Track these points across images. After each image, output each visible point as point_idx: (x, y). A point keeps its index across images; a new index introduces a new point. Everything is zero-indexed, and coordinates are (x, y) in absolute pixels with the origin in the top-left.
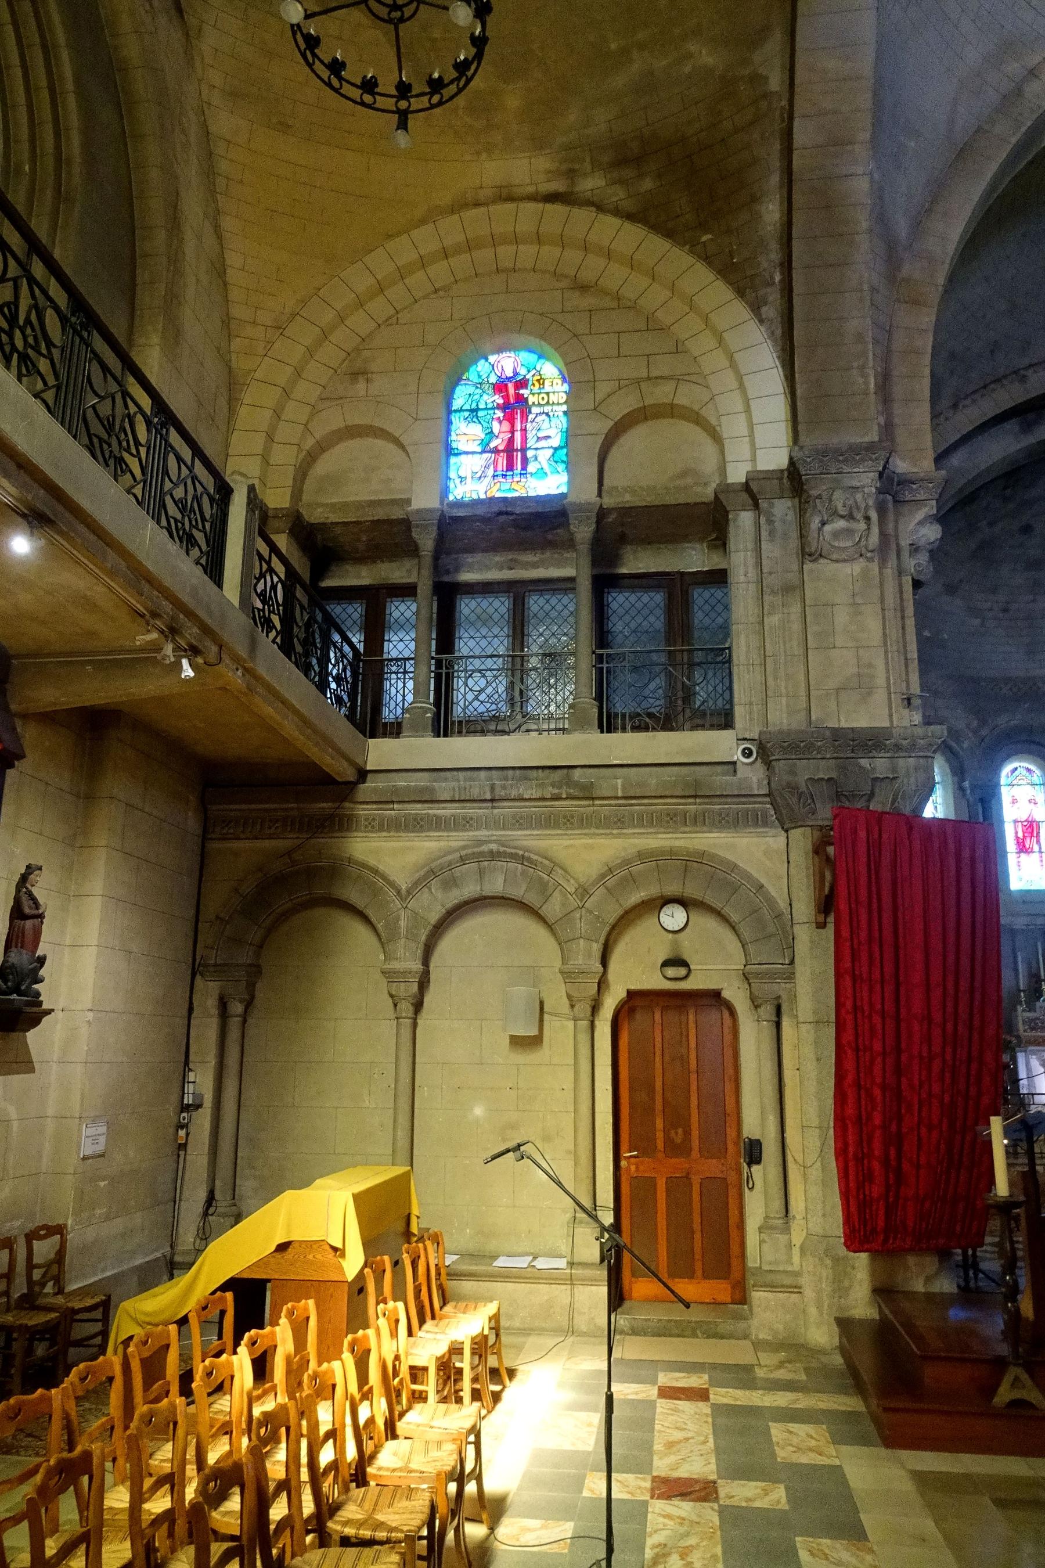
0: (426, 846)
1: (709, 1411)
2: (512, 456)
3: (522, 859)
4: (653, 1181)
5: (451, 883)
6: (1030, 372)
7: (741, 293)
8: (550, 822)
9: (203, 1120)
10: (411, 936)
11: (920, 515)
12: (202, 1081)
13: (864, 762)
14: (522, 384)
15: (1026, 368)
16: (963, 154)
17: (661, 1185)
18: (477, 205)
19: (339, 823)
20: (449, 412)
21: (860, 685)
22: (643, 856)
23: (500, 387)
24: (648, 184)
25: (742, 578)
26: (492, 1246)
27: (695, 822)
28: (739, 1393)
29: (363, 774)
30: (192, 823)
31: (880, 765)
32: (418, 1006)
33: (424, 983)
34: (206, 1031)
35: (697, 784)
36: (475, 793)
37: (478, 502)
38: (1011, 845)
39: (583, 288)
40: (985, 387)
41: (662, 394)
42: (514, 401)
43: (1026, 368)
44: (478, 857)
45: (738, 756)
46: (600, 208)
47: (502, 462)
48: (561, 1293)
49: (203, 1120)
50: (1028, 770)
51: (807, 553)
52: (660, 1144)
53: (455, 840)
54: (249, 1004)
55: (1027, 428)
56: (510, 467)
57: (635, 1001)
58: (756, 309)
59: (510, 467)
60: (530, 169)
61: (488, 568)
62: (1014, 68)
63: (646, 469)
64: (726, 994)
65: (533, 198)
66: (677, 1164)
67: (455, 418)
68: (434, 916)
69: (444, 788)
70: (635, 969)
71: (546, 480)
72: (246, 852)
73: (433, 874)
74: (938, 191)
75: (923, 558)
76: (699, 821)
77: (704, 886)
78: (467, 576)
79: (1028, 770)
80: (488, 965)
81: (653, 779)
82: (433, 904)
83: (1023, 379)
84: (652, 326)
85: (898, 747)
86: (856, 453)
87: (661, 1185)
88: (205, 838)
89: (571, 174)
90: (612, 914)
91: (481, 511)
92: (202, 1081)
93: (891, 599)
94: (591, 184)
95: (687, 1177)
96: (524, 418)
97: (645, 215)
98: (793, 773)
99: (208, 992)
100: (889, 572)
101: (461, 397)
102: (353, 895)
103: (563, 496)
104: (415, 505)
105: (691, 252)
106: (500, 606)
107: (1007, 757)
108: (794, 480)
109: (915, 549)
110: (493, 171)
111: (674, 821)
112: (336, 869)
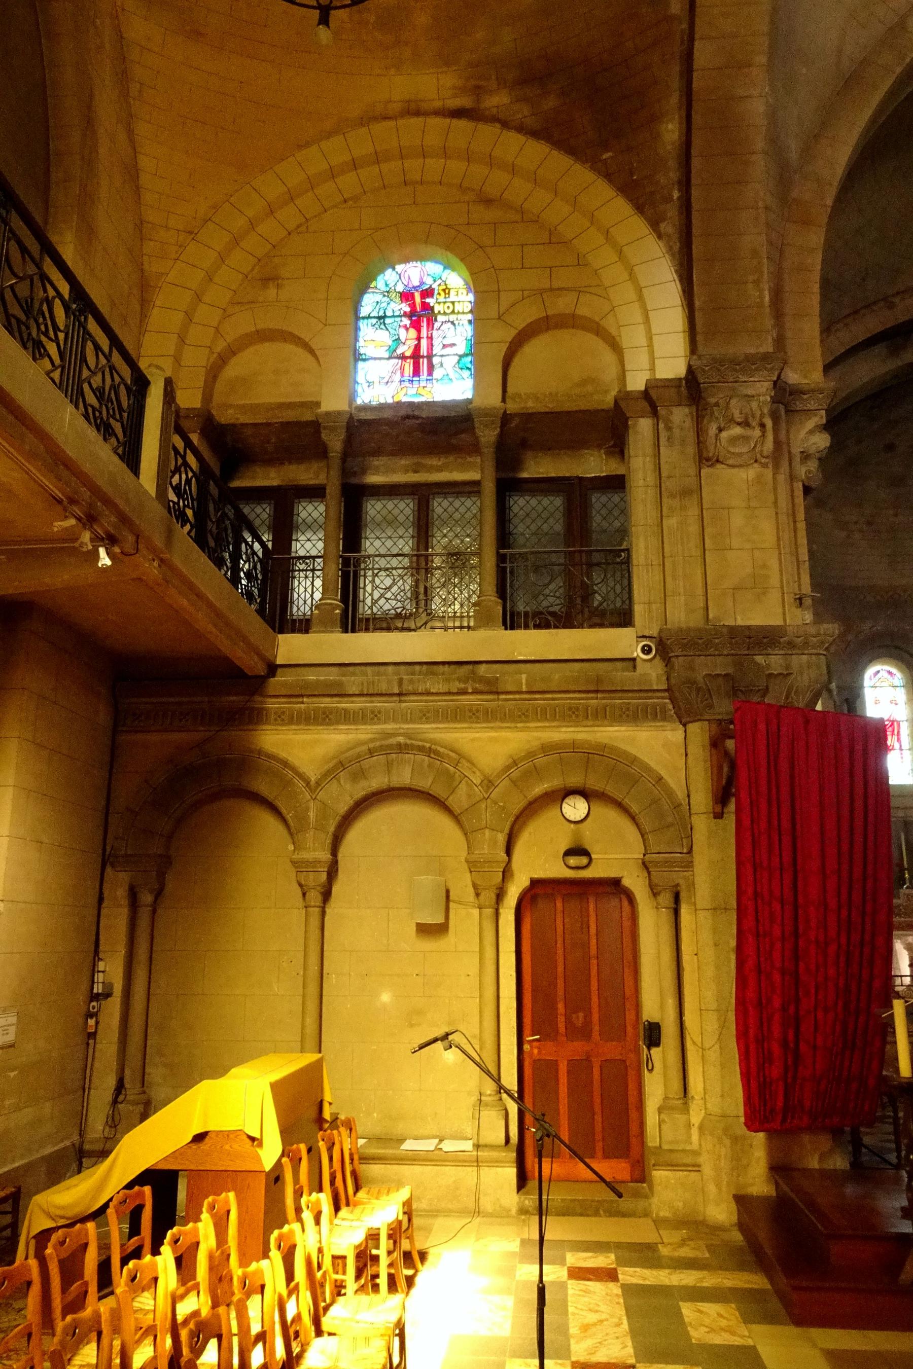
0: (334, 739)
1: (619, 1291)
2: (419, 361)
3: (429, 752)
4: (553, 1066)
5: (359, 775)
6: (897, 300)
7: (640, 209)
8: (457, 716)
9: (112, 1009)
10: (320, 828)
11: (811, 424)
12: (112, 970)
13: (759, 659)
14: (428, 293)
15: (893, 296)
16: (851, 82)
17: (563, 1067)
18: (386, 118)
19: (252, 717)
20: (357, 318)
21: (755, 585)
22: (547, 749)
23: (406, 296)
24: (551, 103)
25: (641, 483)
26: (400, 1128)
27: (596, 716)
28: (647, 1272)
29: (273, 669)
30: (103, 717)
31: (774, 661)
32: (327, 895)
33: (333, 871)
34: (116, 921)
35: (599, 680)
36: (384, 688)
37: (382, 407)
39: (488, 202)
40: (856, 312)
41: (563, 305)
42: (420, 310)
43: (893, 296)
44: (386, 750)
45: (638, 653)
46: (505, 125)
47: (409, 367)
48: (468, 1174)
49: (112, 1009)
50: (890, 673)
51: (705, 458)
52: (562, 1029)
53: (363, 733)
54: (159, 894)
55: (894, 352)
56: (416, 372)
57: (538, 889)
58: (654, 225)
59: (416, 372)
60: (437, 85)
61: (394, 471)
63: (551, 375)
64: (626, 882)
65: (438, 113)
66: (577, 1048)
67: (362, 324)
68: (343, 808)
69: (353, 682)
70: (539, 857)
71: (452, 384)
72: (156, 745)
73: (342, 766)
75: (813, 465)
76: (601, 716)
78: (374, 479)
79: (890, 673)
80: (395, 854)
81: (557, 674)
83: (891, 306)
84: (554, 239)
85: (791, 645)
87: (563, 1067)
88: (115, 731)
89: (478, 91)
90: (517, 804)
91: (387, 414)
92: (112, 970)
93: (783, 503)
95: (588, 1060)
96: (430, 324)
97: (545, 132)
98: (691, 668)
99: (118, 885)
100: (781, 478)
101: (369, 304)
102: (263, 787)
103: (469, 401)
104: (326, 407)
105: (593, 168)
106: (405, 508)
107: (871, 661)
108: (692, 388)
109: (806, 456)
110: (403, 85)
111: (574, 715)
112: (248, 761)
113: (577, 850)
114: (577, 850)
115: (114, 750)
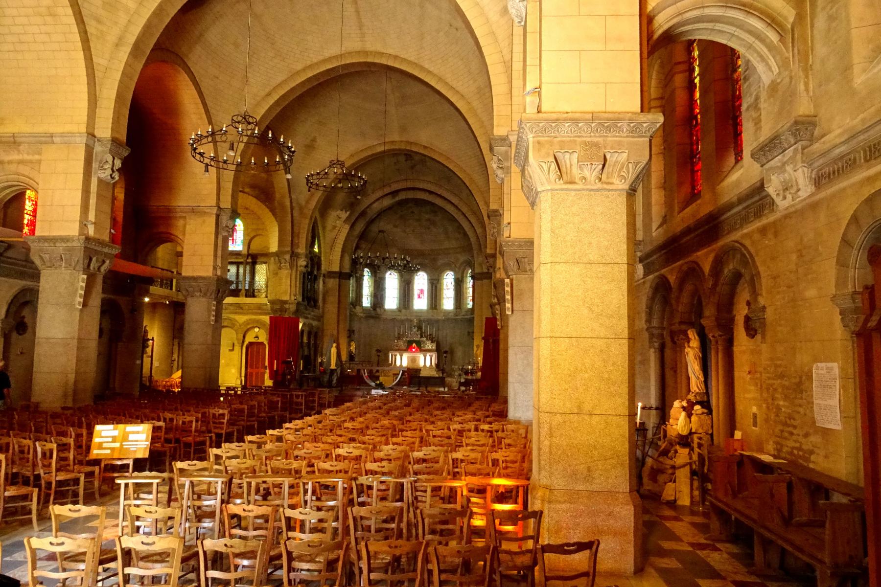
8: (236, 313)
9: (176, 363)
12: (175, 356)
30: (172, 313)
38: (416, 296)
39: (247, 209)
41: (260, 232)
49: (176, 363)
51: (280, 268)
55: (393, 197)
57: (251, 344)
63: (255, 248)
70: (250, 338)
76: (261, 314)
77: (260, 324)
84: (259, 218)
86: (288, 252)
92: (175, 356)
93: (294, 276)
94: (247, 190)
111: (257, 314)
113: (257, 337)
114: (257, 337)
115: (175, 317)
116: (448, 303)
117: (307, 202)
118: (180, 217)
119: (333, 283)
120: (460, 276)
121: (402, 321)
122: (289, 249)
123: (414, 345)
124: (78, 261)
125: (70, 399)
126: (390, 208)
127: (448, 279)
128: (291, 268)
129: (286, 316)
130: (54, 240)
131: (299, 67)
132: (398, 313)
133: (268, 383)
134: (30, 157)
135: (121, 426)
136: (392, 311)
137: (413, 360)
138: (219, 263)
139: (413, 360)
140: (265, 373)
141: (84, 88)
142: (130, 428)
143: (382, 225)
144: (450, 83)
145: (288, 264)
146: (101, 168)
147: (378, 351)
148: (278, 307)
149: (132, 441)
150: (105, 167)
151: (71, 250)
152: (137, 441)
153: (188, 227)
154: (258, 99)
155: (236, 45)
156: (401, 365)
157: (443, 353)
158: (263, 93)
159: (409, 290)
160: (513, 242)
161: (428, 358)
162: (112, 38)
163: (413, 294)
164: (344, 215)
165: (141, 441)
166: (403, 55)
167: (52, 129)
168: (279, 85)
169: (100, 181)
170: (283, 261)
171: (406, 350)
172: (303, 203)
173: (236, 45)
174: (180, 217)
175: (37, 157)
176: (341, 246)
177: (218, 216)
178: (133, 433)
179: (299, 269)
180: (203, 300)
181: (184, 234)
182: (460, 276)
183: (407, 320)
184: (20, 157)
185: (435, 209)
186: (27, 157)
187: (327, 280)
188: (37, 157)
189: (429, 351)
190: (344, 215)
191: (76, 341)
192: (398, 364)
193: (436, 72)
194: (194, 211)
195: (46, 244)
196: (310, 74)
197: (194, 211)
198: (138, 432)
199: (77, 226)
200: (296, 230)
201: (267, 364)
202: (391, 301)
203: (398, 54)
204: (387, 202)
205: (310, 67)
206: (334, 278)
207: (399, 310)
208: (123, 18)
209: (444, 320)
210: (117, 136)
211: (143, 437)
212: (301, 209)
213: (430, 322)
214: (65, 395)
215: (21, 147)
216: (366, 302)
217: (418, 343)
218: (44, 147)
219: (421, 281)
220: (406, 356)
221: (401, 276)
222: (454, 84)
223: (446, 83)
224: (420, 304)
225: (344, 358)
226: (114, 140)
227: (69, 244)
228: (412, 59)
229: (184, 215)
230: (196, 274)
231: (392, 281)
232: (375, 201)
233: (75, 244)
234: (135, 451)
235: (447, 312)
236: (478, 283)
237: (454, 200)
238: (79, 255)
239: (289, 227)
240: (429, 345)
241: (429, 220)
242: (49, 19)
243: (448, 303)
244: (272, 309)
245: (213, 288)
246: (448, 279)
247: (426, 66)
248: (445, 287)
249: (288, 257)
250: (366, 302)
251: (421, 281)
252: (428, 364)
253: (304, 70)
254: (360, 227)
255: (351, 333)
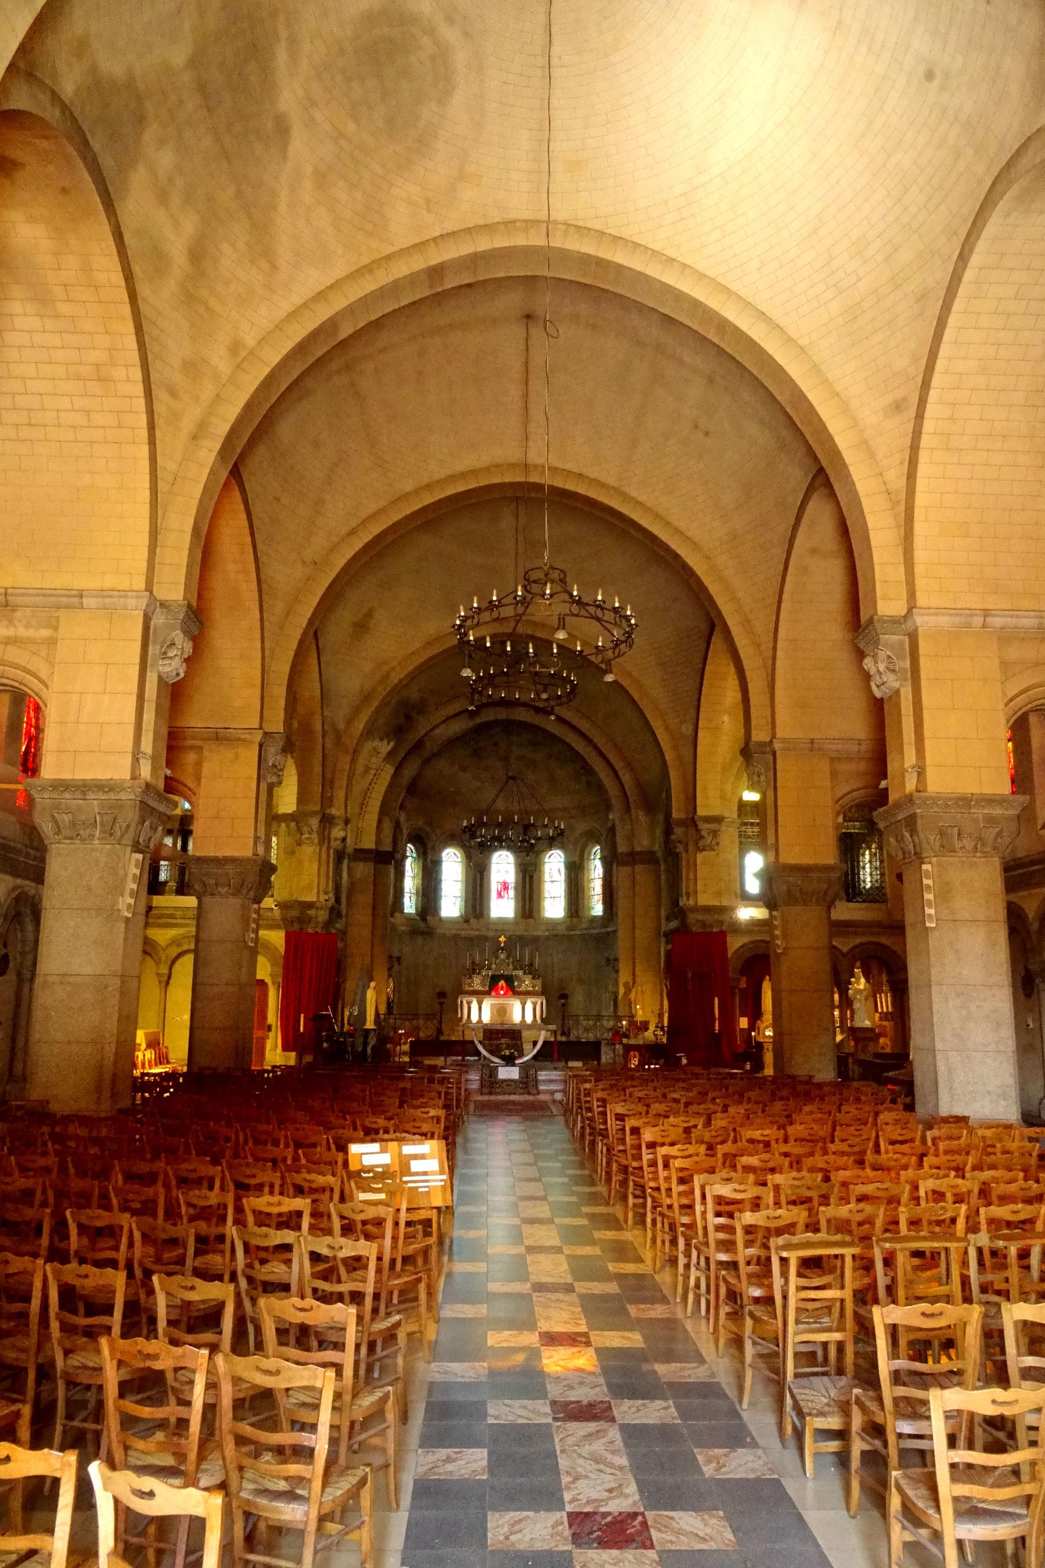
0: (173, 932)
16: (367, 698)
21: (309, 887)
31: (311, 912)
32: (167, 983)
33: (169, 977)
38: (494, 894)
62: (386, 668)
68: (174, 955)
69: (179, 913)
73: (175, 942)
74: (356, 711)
82: (174, 951)
86: (314, 814)
100: (324, 849)
109: (336, 839)
116: (554, 906)
117: (350, 722)
118: (191, 748)
119: (364, 870)
120: (577, 859)
121: (470, 940)
122: (318, 808)
123: (502, 983)
124: (128, 826)
125: (107, 1093)
126: (459, 739)
127: (554, 865)
128: (321, 843)
129: (310, 930)
130: (84, 788)
131: (408, 486)
132: (465, 925)
133: (275, 1054)
134: (31, 633)
135: (393, 1145)
136: (451, 921)
137: (501, 1011)
138: (262, 833)
139: (501, 1011)
140: (267, 1037)
141: (145, 510)
142: (408, 1149)
143: (442, 765)
144: (675, 523)
145: (315, 836)
146: (164, 655)
147: (442, 995)
148: (295, 913)
149: (417, 1174)
150: (171, 654)
151: (119, 805)
152: (425, 1173)
153: (206, 768)
154: (336, 539)
155: (316, 444)
156: (480, 1021)
157: (557, 1001)
158: (345, 530)
159: (481, 885)
160: (934, 799)
161: (529, 1006)
162: (187, 425)
163: (489, 891)
164: (385, 747)
165: (433, 1173)
166: (593, 473)
167: (80, 582)
168: (373, 516)
169: (160, 679)
170: (305, 829)
171: (488, 993)
172: (341, 726)
173: (316, 444)
174: (191, 748)
175: (45, 633)
176: (379, 804)
177: (261, 745)
178: (416, 1157)
179: (334, 844)
180: (235, 902)
181: (198, 778)
182: (577, 859)
183: (479, 937)
184: (11, 632)
185: (539, 737)
186: (22, 632)
187: (353, 864)
188: (45, 633)
189: (528, 993)
190: (385, 747)
191: (118, 981)
192: (474, 1018)
193: (648, 504)
194: (219, 737)
195: (67, 795)
196: (428, 499)
197: (219, 737)
198: (423, 1157)
199: (128, 760)
200: (328, 776)
201: (273, 1017)
202: (451, 905)
203: (584, 471)
204: (458, 727)
205: (428, 487)
206: (365, 860)
207: (465, 919)
208: (208, 392)
209: (547, 938)
210: (189, 596)
211: (432, 1165)
212: (338, 735)
213: (520, 938)
214: (99, 1089)
215: (19, 614)
216: (409, 906)
217: (509, 980)
218: (62, 614)
219: (503, 866)
220: (487, 1004)
221: (469, 857)
222: (682, 525)
223: (668, 524)
224: (502, 908)
225: (383, 1009)
226: (189, 606)
227: (112, 796)
228: (611, 481)
229: (199, 743)
230: (220, 854)
231: (452, 865)
232: (443, 724)
233: (123, 796)
234: (428, 1193)
235: (553, 923)
236: (622, 874)
237: (584, 726)
238: (131, 815)
239: (318, 769)
240: (527, 983)
241: (521, 758)
242: (94, 387)
243: (554, 906)
244: (284, 919)
245: (253, 878)
246: (554, 865)
247: (634, 494)
248: (547, 877)
249: (315, 822)
250: (409, 906)
251: (503, 866)
252: (529, 1019)
253: (417, 492)
254: (410, 770)
255: (394, 961)
